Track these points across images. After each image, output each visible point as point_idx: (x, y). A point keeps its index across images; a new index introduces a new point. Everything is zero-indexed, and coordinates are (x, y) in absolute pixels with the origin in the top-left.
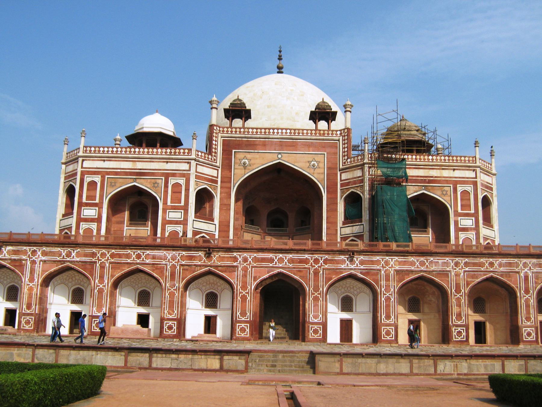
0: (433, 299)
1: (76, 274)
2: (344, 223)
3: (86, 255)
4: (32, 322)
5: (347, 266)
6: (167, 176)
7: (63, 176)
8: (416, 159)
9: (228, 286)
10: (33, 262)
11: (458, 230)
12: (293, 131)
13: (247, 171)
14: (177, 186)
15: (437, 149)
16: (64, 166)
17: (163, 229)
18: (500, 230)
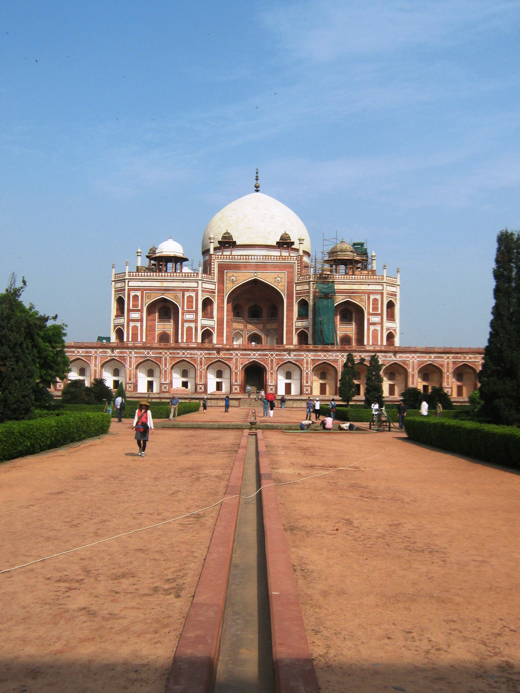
0: (333, 372)
1: (150, 362)
2: (297, 319)
3: (157, 353)
4: (132, 387)
5: (287, 357)
6: (184, 290)
7: (113, 290)
8: (344, 278)
9: (228, 367)
10: (131, 357)
11: (370, 324)
12: (264, 257)
13: (234, 285)
14: (190, 297)
15: (372, 256)
16: (113, 283)
17: (183, 326)
18: (400, 322)
